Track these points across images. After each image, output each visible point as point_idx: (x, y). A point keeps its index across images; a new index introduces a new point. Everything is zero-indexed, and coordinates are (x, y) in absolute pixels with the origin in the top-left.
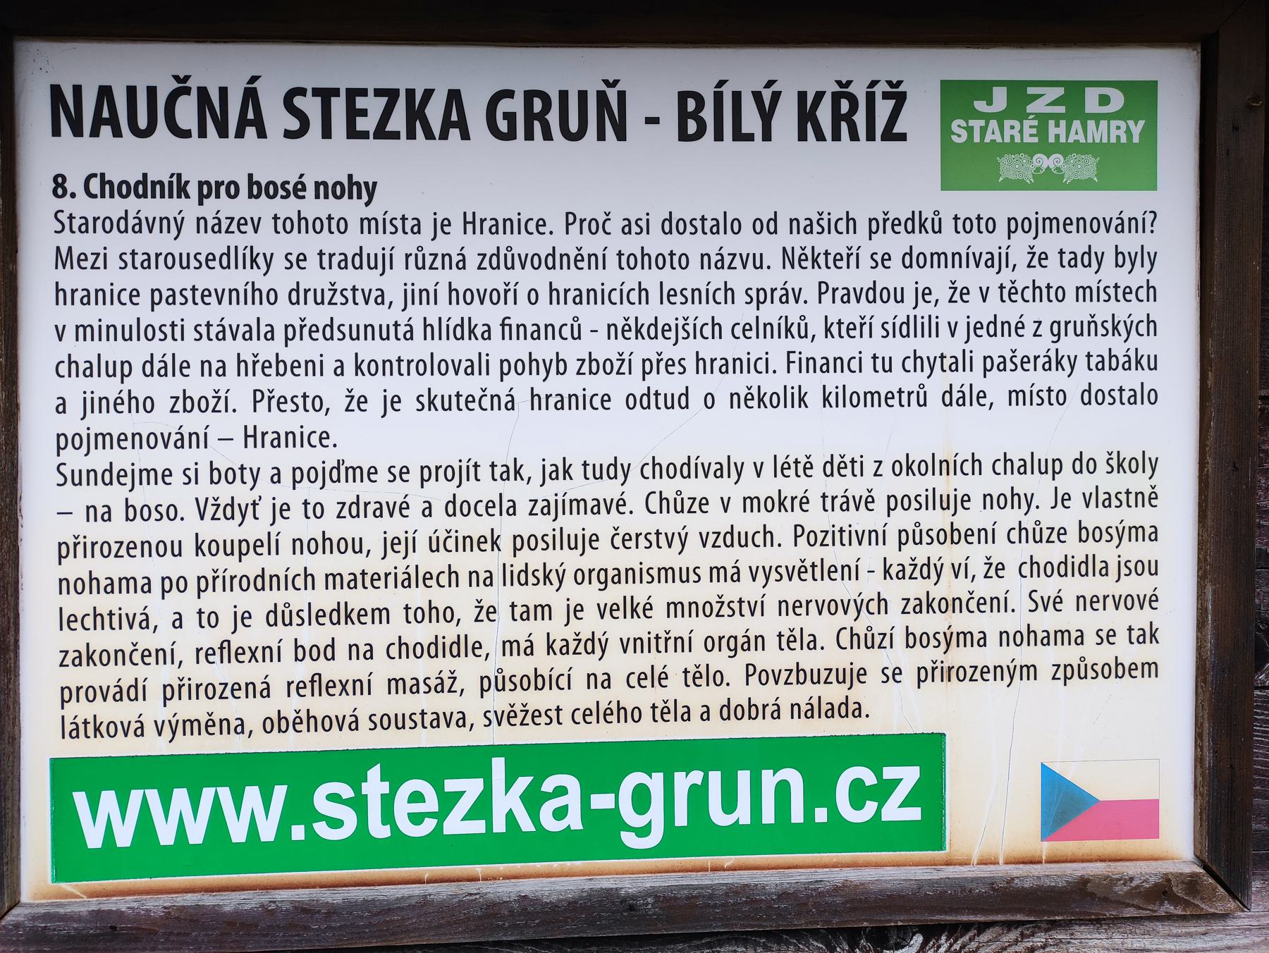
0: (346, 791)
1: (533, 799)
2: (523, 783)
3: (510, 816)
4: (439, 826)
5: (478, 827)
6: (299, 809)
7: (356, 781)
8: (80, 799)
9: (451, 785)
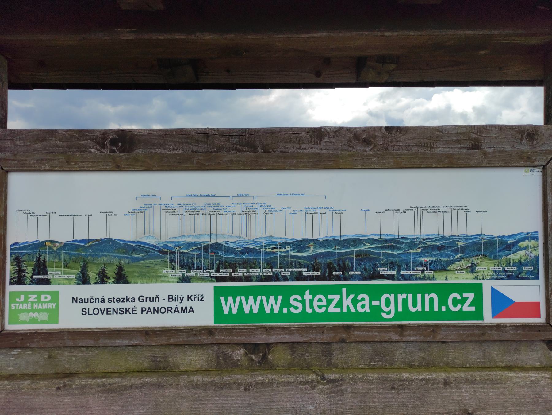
0: (299, 298)
1: (355, 302)
2: (352, 296)
3: (348, 307)
4: (327, 310)
5: (338, 310)
6: (286, 303)
7: (302, 294)
8: (222, 299)
9: (330, 297)
